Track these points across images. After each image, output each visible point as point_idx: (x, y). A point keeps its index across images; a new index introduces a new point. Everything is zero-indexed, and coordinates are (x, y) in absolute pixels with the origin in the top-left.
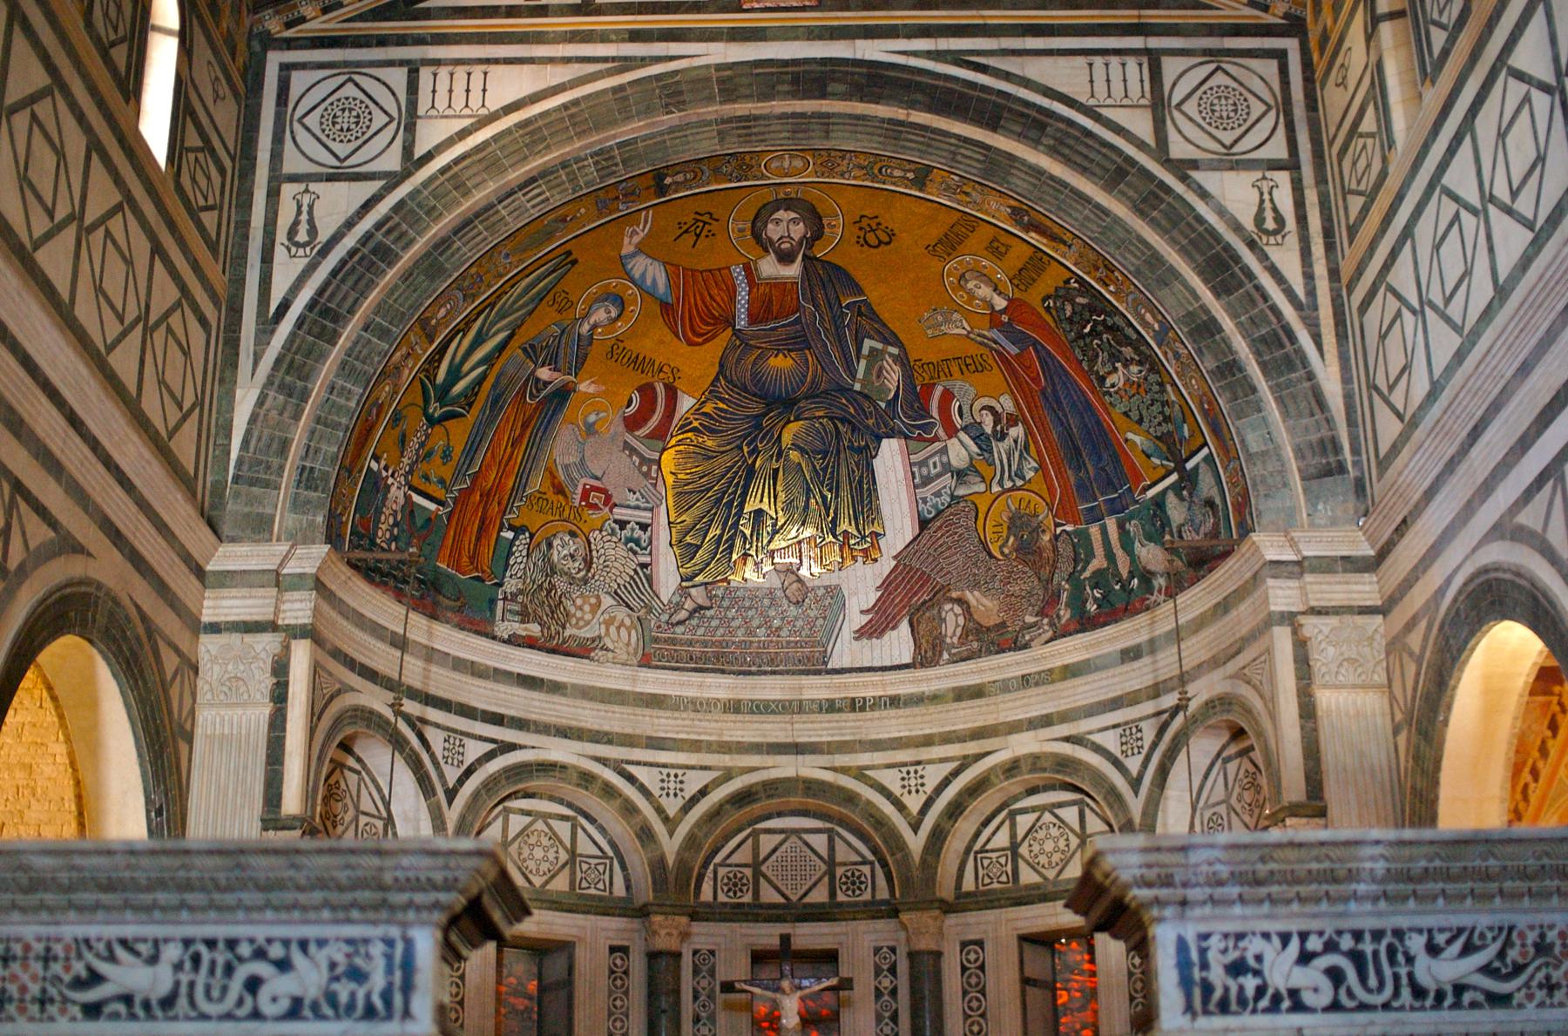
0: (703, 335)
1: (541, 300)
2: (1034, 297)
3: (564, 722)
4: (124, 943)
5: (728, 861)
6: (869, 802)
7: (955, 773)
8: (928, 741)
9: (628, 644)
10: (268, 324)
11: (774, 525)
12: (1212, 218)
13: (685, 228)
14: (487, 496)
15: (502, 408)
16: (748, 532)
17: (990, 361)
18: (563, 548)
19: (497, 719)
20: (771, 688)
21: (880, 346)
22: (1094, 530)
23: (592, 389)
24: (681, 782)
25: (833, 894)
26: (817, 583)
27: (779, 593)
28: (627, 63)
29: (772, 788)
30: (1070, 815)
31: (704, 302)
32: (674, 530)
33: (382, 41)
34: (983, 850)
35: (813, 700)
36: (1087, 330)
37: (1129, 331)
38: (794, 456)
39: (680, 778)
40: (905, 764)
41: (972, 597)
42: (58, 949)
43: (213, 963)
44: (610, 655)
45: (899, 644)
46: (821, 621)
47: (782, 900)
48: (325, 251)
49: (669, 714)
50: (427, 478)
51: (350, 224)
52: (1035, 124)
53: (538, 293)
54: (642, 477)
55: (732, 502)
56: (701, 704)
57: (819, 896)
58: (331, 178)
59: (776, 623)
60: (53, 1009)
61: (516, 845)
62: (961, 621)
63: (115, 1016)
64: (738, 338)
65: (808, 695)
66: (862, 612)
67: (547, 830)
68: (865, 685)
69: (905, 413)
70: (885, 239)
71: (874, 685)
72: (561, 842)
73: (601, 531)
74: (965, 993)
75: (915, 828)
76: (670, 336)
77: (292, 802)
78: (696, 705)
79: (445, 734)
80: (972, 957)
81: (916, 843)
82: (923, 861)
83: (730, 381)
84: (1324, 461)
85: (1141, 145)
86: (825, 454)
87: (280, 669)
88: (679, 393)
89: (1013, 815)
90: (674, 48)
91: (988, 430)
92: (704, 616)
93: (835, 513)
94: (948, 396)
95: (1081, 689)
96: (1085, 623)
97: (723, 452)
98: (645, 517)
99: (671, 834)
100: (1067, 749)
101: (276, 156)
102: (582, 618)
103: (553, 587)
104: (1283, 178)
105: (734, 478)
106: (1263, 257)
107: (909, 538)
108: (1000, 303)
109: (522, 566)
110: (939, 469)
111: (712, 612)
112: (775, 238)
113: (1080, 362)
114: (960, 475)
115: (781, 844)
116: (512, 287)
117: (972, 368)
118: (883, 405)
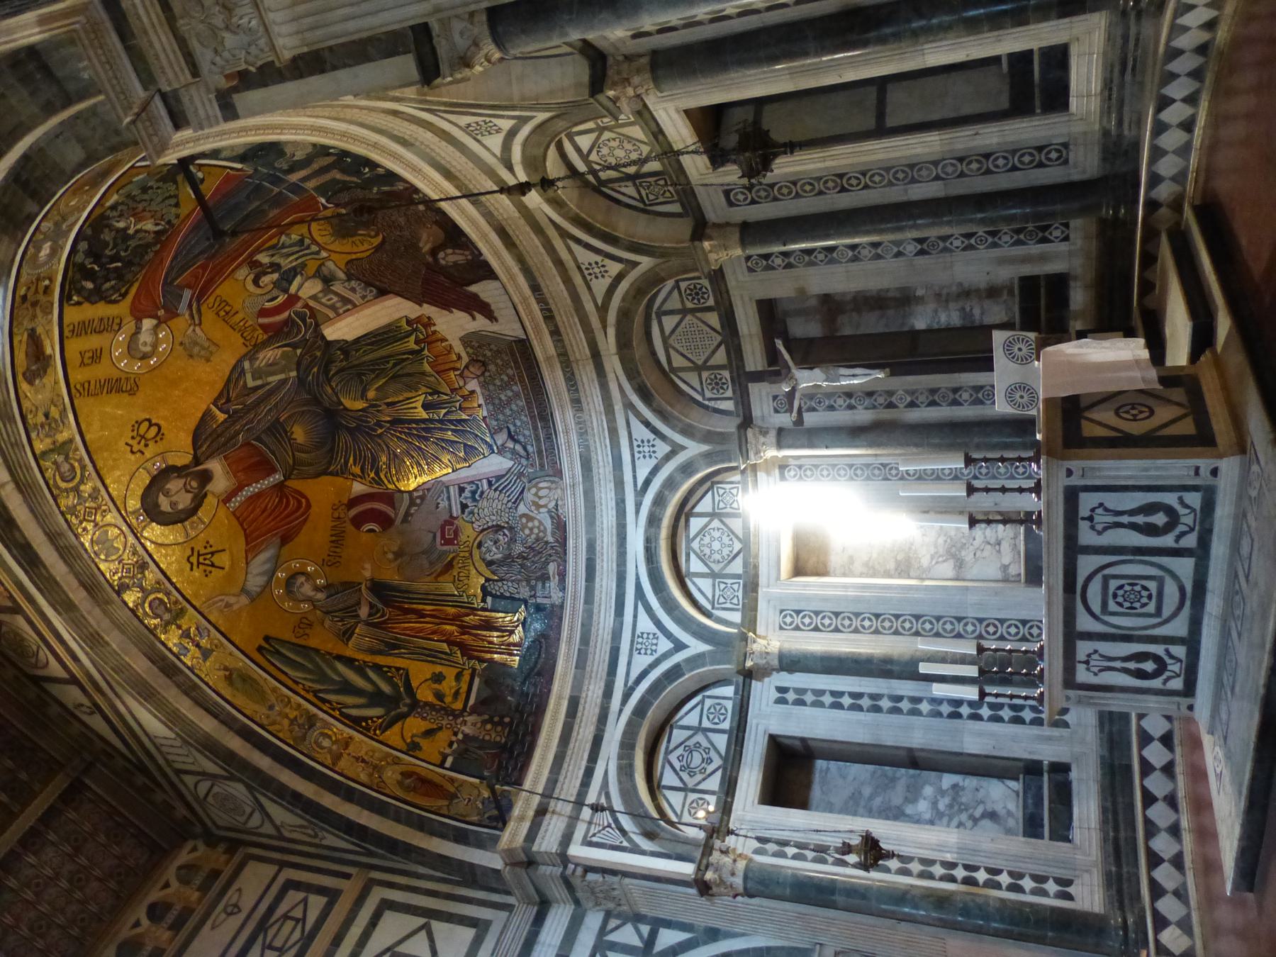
0: (297, 499)
1: (304, 647)
2: (123, 308)
3: (615, 539)
5: (700, 390)
6: (623, 300)
7: (578, 241)
8: (559, 263)
9: (549, 488)
11: (431, 394)
13: (210, 568)
14: (465, 629)
15: (396, 639)
16: (444, 411)
17: (211, 300)
21: (249, 376)
22: (310, 185)
23: (368, 566)
24: (643, 441)
25: (709, 309)
26: (464, 354)
27: (482, 379)
29: (632, 373)
31: (270, 515)
32: (458, 466)
34: (642, 200)
35: (555, 347)
36: (119, 264)
37: (83, 246)
38: (371, 394)
39: (640, 443)
40: (584, 277)
41: (426, 247)
44: (560, 503)
46: (492, 346)
47: (723, 347)
49: (593, 454)
50: (456, 694)
53: (297, 653)
54: (426, 502)
55: (423, 429)
56: (580, 429)
57: (713, 319)
59: (506, 378)
61: (712, 565)
62: (449, 251)
64: (291, 474)
65: (552, 350)
66: (474, 318)
67: (698, 539)
68: (530, 312)
69: (297, 334)
70: (146, 424)
71: (528, 306)
72: (706, 526)
73: (473, 523)
74: (775, 199)
75: (635, 264)
76: (308, 524)
79: (635, 653)
80: (741, 197)
81: (646, 262)
82: (662, 255)
83: (330, 464)
84: (39, 76)
86: (360, 375)
88: (352, 497)
91: (276, 276)
92: (515, 432)
93: (404, 354)
94: (264, 313)
95: (459, 167)
97: (388, 447)
98: (454, 491)
99: (683, 448)
102: (538, 528)
103: (520, 556)
105: (405, 433)
107: (399, 299)
108: (148, 324)
109: (510, 584)
110: (332, 296)
111: (512, 428)
112: (190, 496)
113: (157, 253)
114: (327, 280)
115: (677, 351)
116: (297, 683)
117: (227, 308)
118: (299, 351)
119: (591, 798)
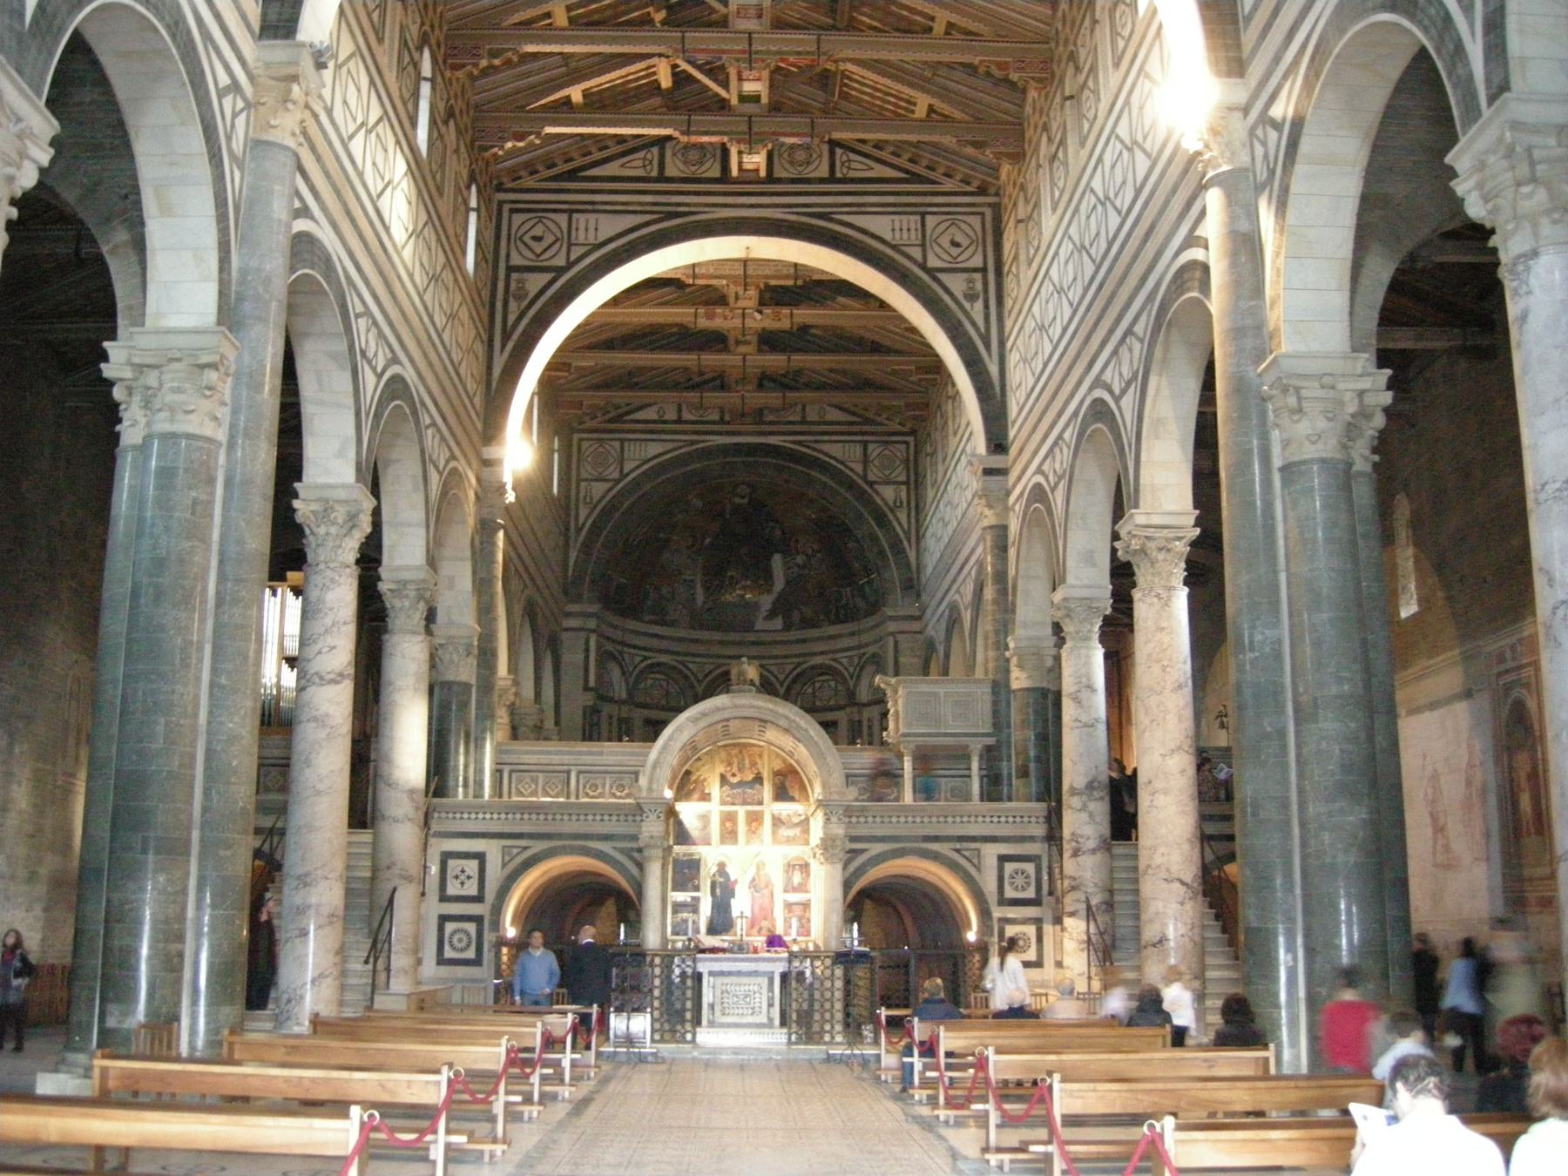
8: (786, 657)
10: (579, 530)
12: (879, 501)
18: (664, 591)
19: (645, 649)
20: (732, 636)
28: (692, 443)
30: (833, 684)
33: (611, 431)
45: (778, 623)
48: (595, 507)
51: (603, 497)
52: (824, 467)
58: (597, 480)
75: (782, 685)
77: (592, 683)
78: (711, 642)
85: (858, 475)
87: (587, 642)
89: (814, 683)
90: (708, 437)
91: (810, 552)
96: (839, 621)
100: (832, 663)
101: (578, 474)
104: (904, 488)
106: (895, 516)
114: (804, 567)
119: (625, 649)
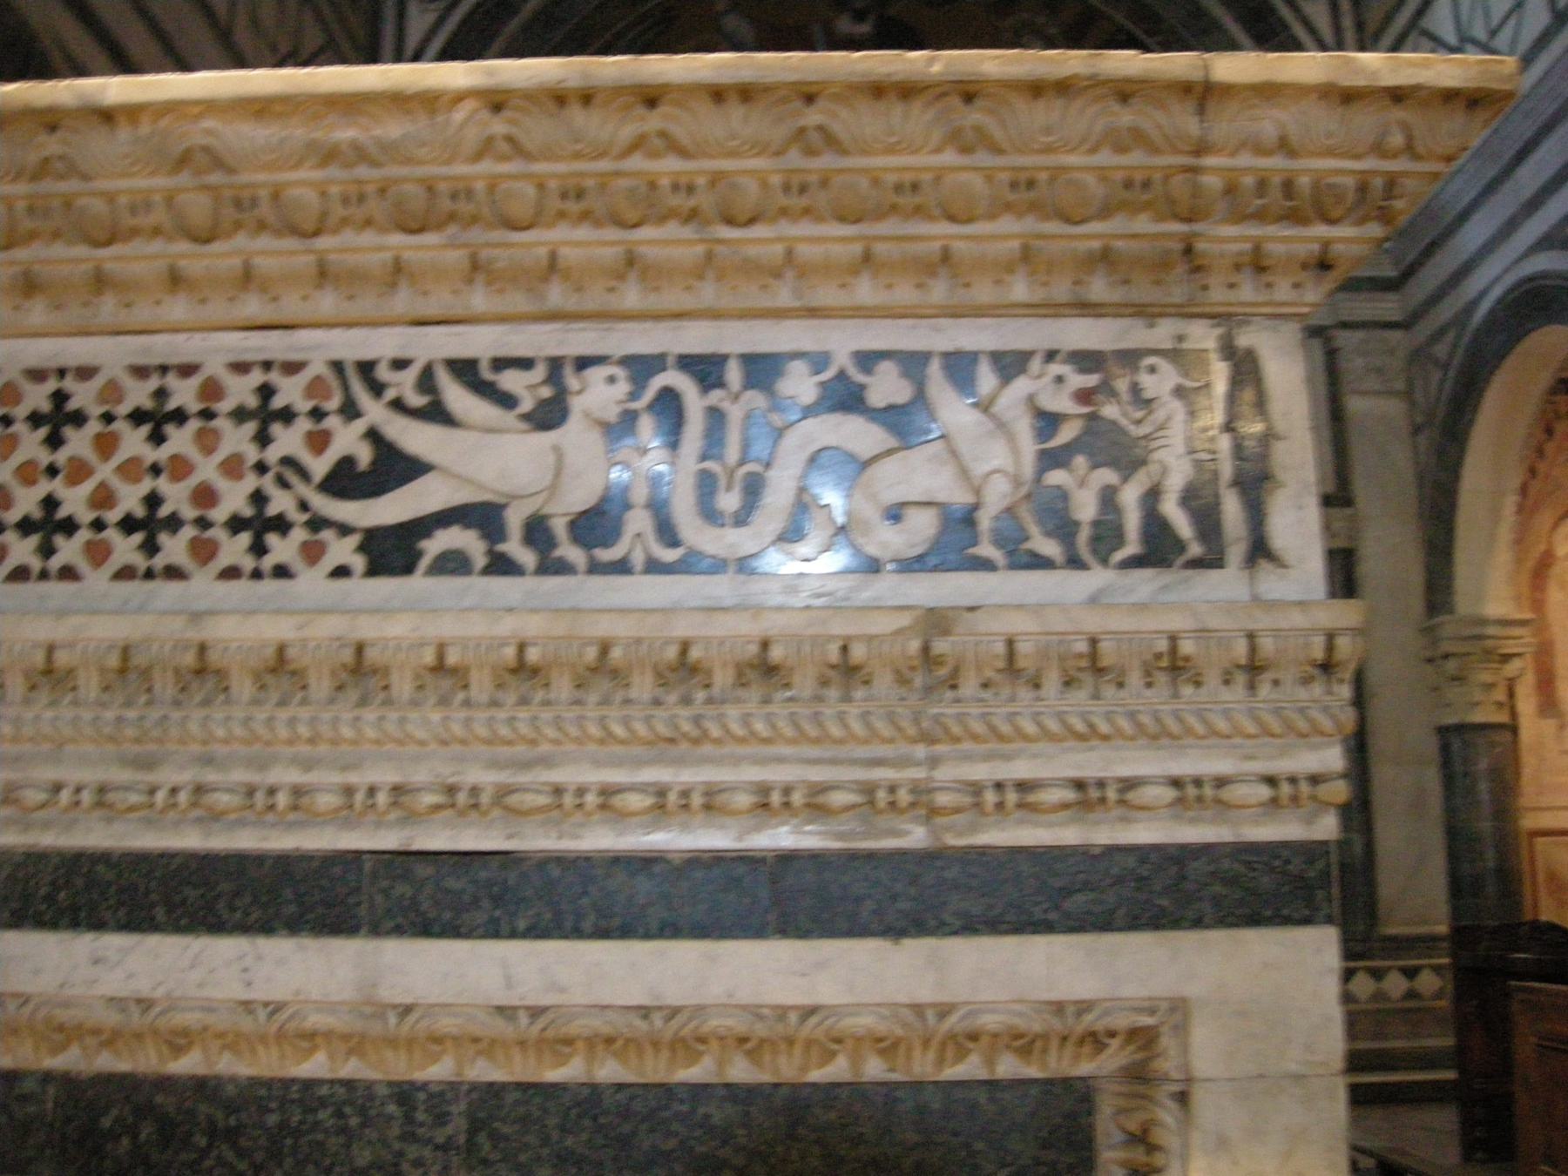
4: (464, 370)
42: (290, 392)
43: (716, 416)
60: (282, 549)
63: (451, 563)
